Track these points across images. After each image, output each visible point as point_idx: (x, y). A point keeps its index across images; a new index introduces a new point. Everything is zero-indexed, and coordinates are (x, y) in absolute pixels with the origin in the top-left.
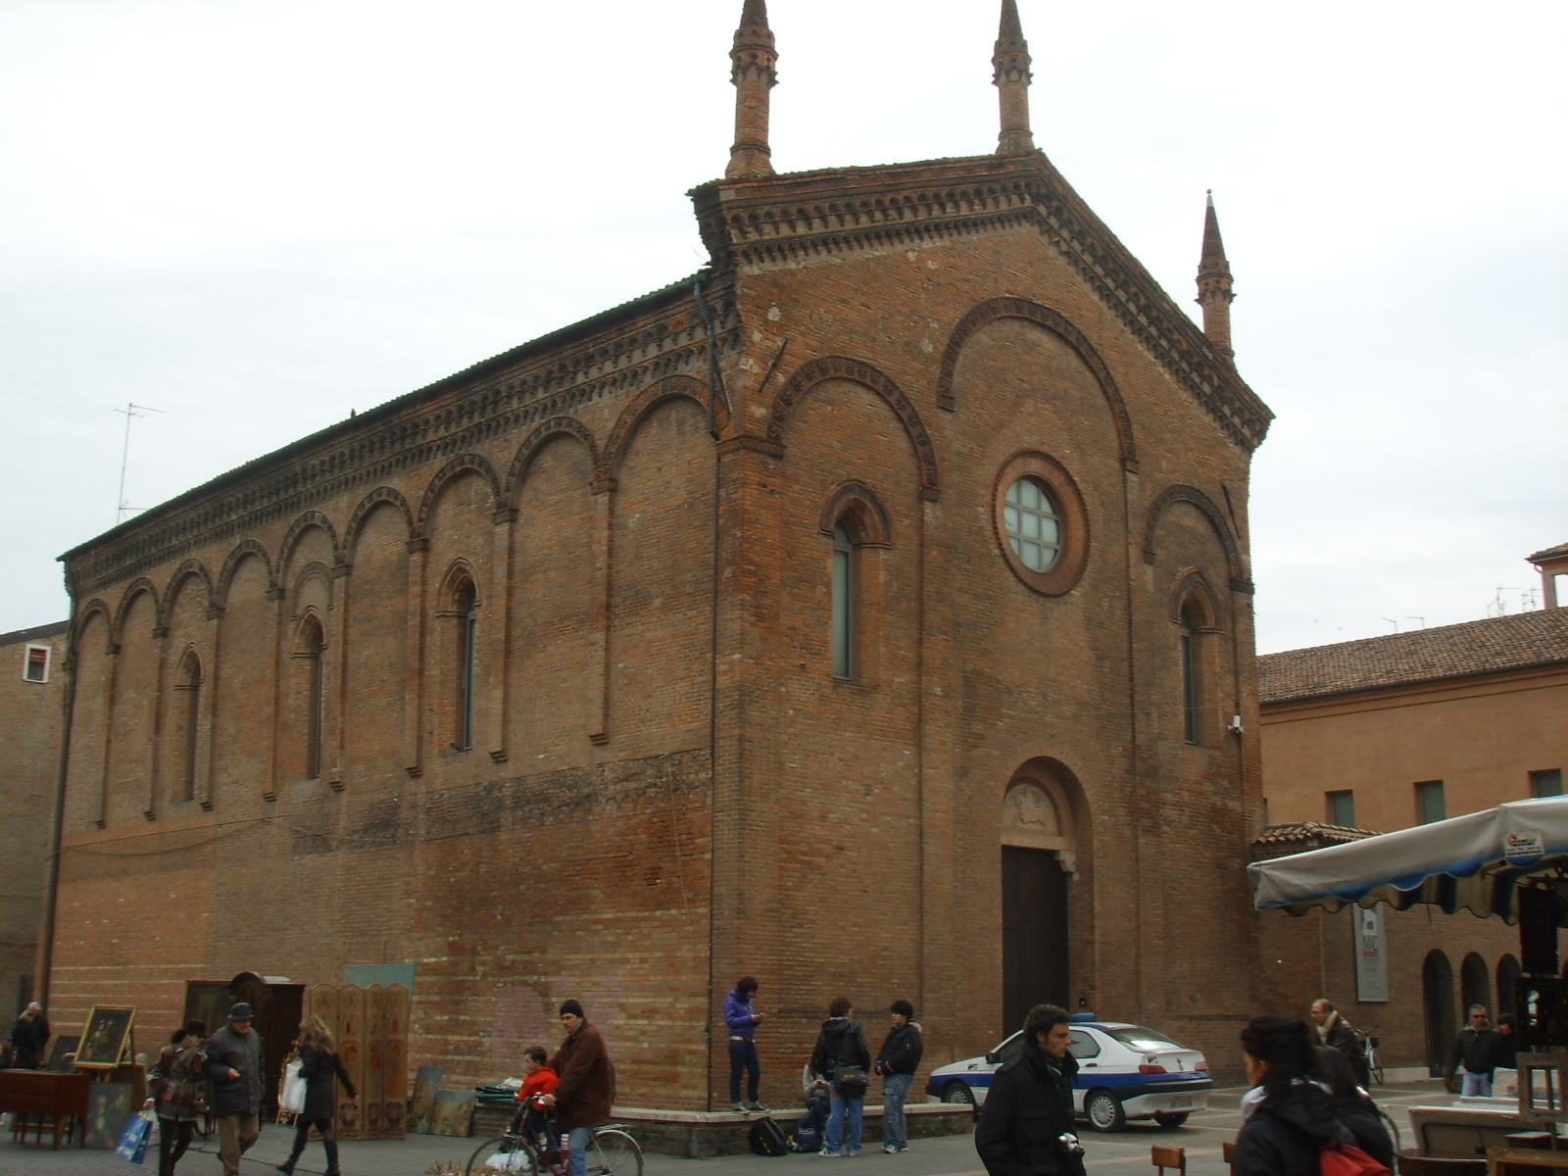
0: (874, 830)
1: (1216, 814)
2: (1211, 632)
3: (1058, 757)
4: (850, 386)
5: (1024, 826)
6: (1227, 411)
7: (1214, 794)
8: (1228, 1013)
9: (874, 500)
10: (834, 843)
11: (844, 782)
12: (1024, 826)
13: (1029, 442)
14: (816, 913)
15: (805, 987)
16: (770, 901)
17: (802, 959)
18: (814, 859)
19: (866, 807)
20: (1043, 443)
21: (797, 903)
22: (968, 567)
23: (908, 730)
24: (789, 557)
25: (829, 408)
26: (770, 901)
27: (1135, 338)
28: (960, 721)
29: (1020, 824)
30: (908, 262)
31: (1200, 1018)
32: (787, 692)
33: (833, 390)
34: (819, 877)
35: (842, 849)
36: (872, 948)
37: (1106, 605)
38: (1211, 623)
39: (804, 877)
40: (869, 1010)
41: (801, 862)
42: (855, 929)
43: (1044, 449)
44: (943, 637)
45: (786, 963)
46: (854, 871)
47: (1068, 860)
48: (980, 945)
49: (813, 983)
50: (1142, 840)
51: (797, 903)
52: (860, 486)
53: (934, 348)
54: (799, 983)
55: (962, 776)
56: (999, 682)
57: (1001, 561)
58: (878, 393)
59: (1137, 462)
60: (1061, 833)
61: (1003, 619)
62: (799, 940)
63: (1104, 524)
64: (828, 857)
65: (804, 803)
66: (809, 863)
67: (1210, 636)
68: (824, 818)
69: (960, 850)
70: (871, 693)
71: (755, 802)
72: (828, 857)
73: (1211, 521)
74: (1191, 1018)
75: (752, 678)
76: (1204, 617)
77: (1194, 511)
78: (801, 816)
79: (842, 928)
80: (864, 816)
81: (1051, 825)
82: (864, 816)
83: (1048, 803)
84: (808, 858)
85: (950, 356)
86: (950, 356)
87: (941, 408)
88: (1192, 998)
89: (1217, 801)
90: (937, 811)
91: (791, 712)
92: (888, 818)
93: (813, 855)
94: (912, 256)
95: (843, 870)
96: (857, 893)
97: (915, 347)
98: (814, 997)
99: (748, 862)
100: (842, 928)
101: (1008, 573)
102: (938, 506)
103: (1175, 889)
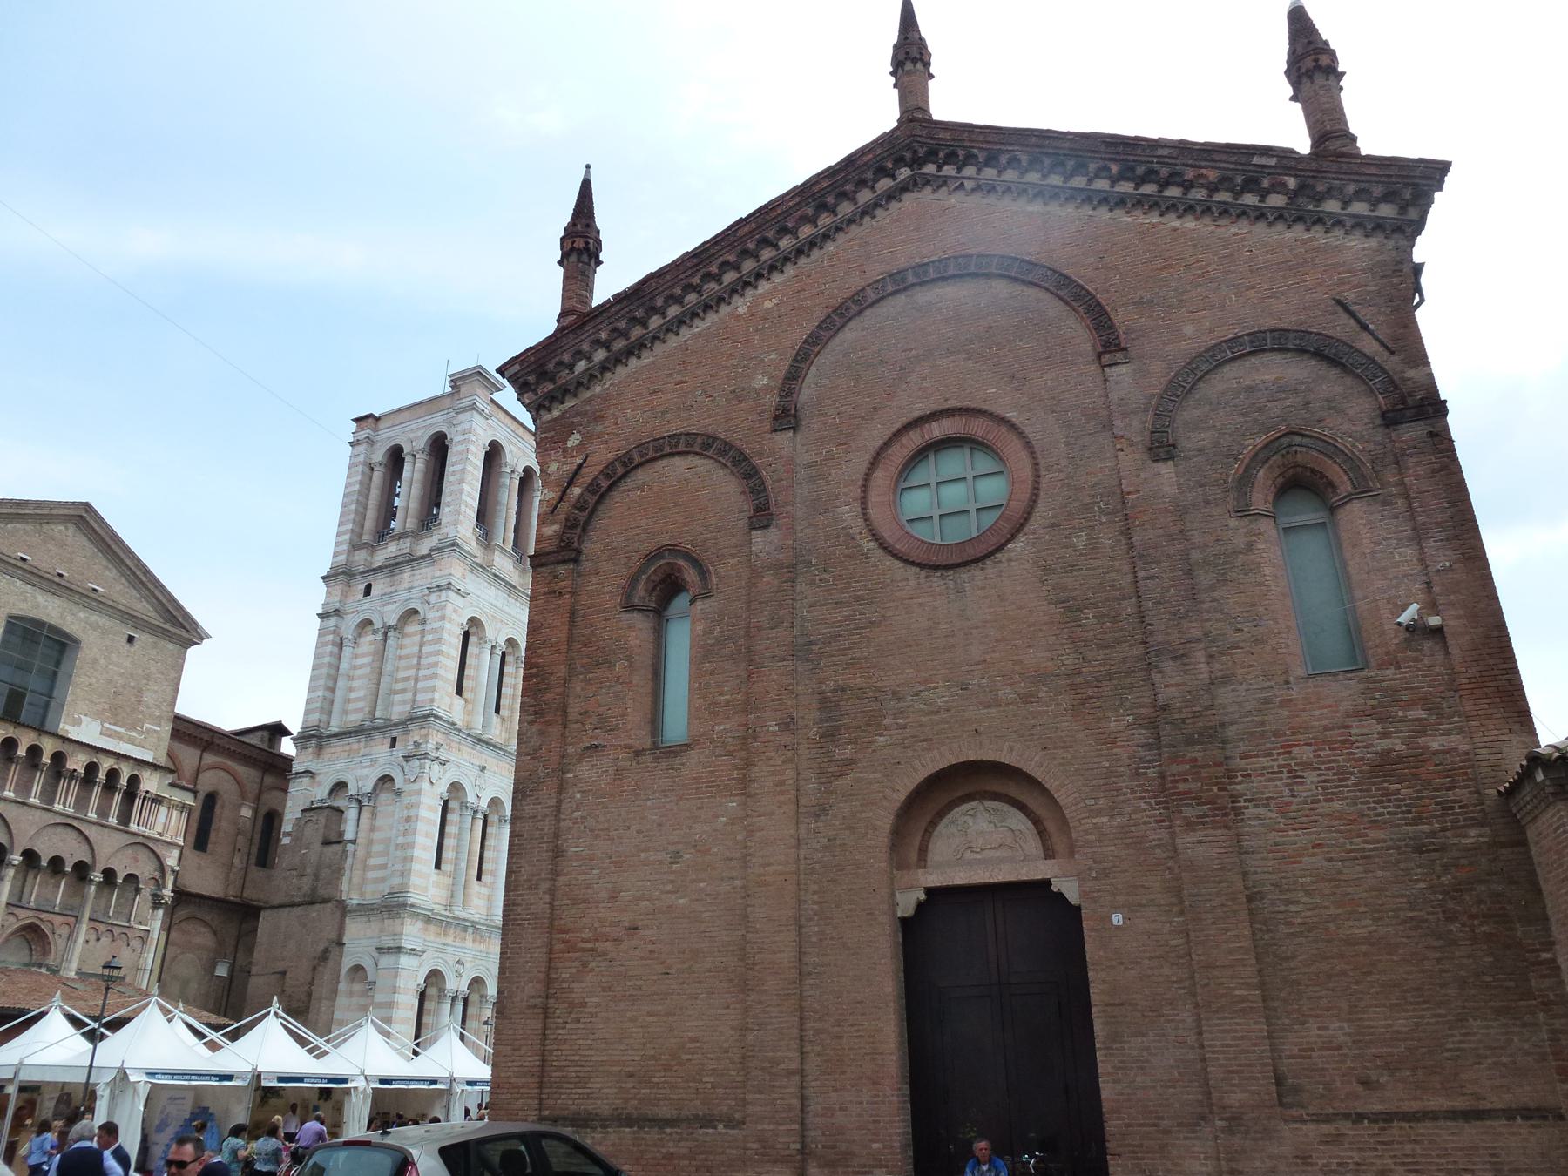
0: (681, 901)
1: (1385, 767)
2: (1347, 500)
3: (991, 756)
4: (665, 462)
5: (978, 856)
6: (1332, 206)
7: (1385, 735)
8: (1486, 1105)
9: (687, 556)
10: (627, 924)
11: (642, 855)
12: (978, 856)
13: (920, 409)
14: (598, 1005)
15: (580, 1091)
16: (533, 997)
17: (577, 1058)
18: (597, 944)
19: (672, 877)
20: (946, 400)
21: (574, 995)
22: (825, 576)
23: (734, 779)
24: (585, 646)
25: (639, 493)
26: (533, 997)
27: (1119, 212)
28: (812, 751)
29: (968, 855)
30: (738, 317)
31: (1388, 1117)
32: (575, 776)
33: (641, 476)
34: (605, 963)
35: (636, 929)
36: (673, 1040)
37: (1080, 541)
38: (1345, 487)
39: (585, 966)
40: (669, 1116)
41: (583, 950)
42: (651, 1019)
43: (953, 403)
44: (780, 664)
45: (555, 1064)
46: (651, 952)
47: (1070, 889)
48: (852, 1025)
49: (590, 1085)
50: (1185, 840)
51: (574, 995)
52: (673, 549)
53: (771, 377)
54: (572, 1086)
55: (819, 816)
56: (878, 689)
57: (879, 553)
58: (697, 454)
59: (1125, 349)
60: (1049, 854)
61: (883, 616)
62: (574, 1037)
63: (1067, 444)
64: (617, 940)
65: (588, 887)
66: (591, 950)
67: (1348, 507)
68: (613, 898)
69: (815, 907)
70: (681, 751)
71: (522, 895)
72: (617, 940)
73: (1318, 354)
74: (1360, 1118)
75: (528, 773)
76: (1331, 484)
77: (1276, 358)
78: (584, 901)
79: (633, 1020)
80: (669, 887)
81: (1032, 845)
82: (669, 887)
83: (1021, 816)
84: (589, 945)
85: (794, 376)
86: (794, 376)
87: (776, 431)
88: (1366, 1083)
89: (1397, 744)
90: (769, 865)
91: (578, 796)
92: (702, 885)
93: (597, 940)
94: (742, 310)
95: (637, 953)
96: (655, 978)
97: (744, 389)
98: (589, 1102)
99: (509, 958)
100: (633, 1020)
101: (889, 562)
102: (772, 529)
103: (1289, 902)
